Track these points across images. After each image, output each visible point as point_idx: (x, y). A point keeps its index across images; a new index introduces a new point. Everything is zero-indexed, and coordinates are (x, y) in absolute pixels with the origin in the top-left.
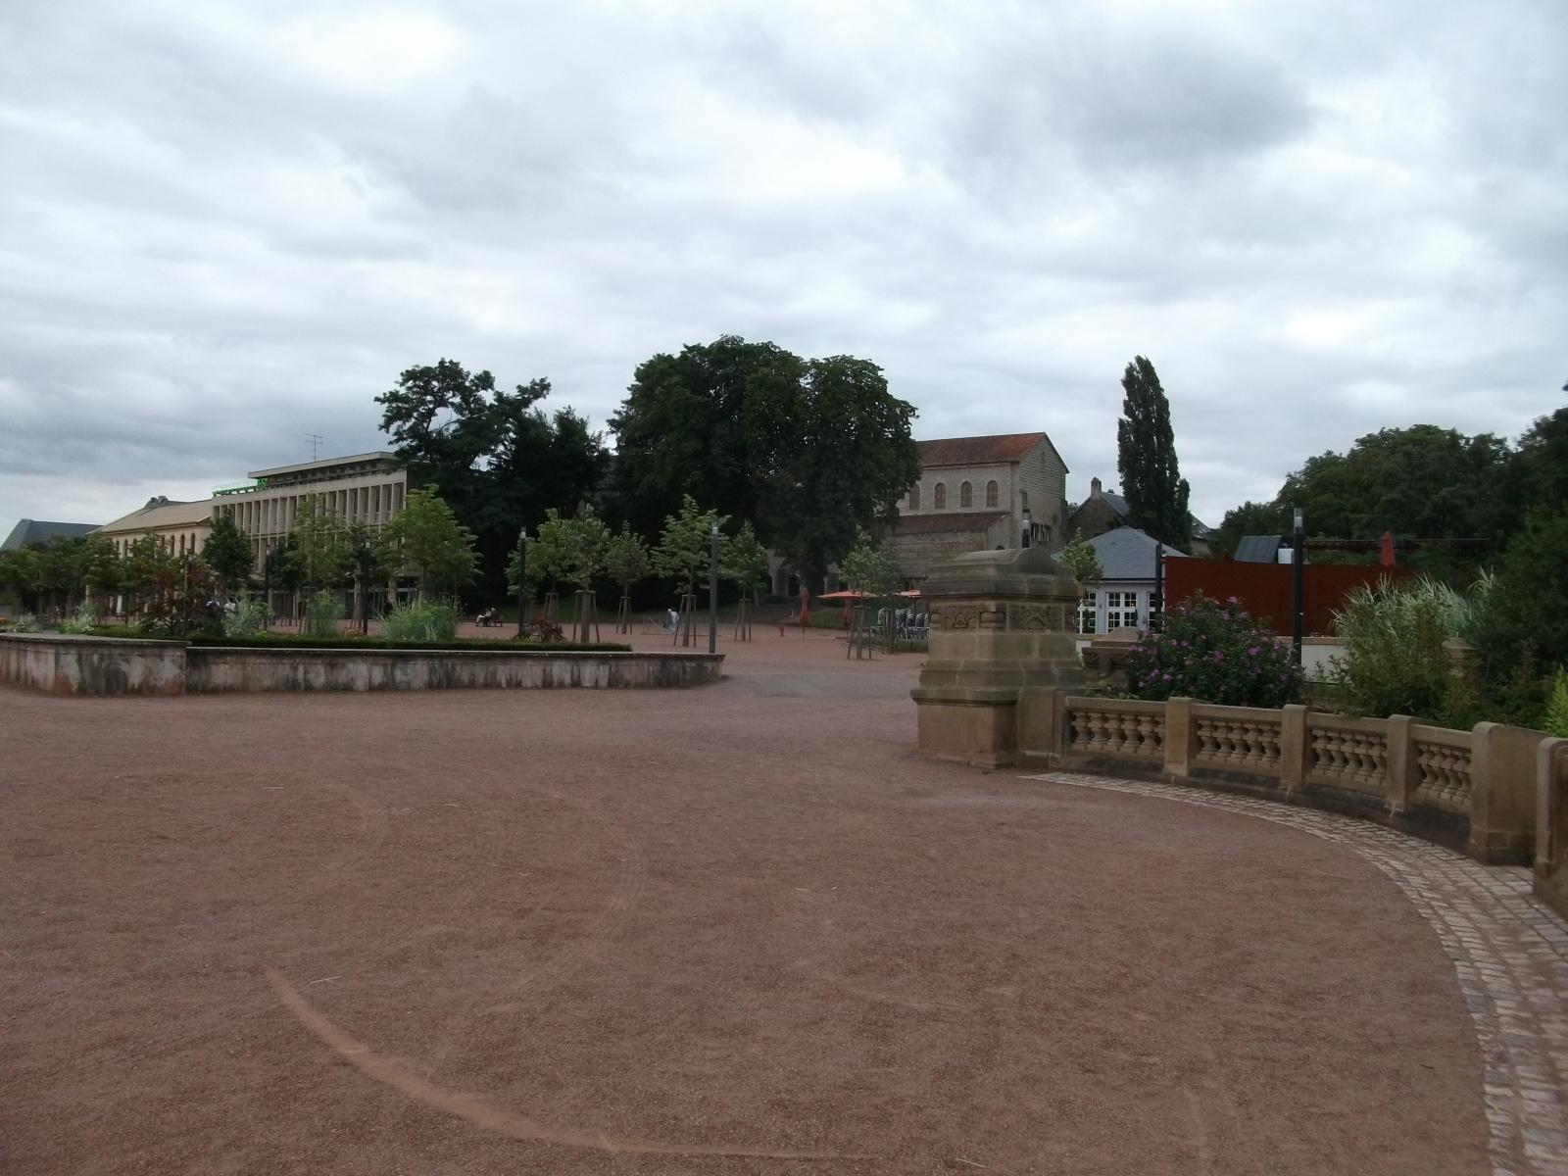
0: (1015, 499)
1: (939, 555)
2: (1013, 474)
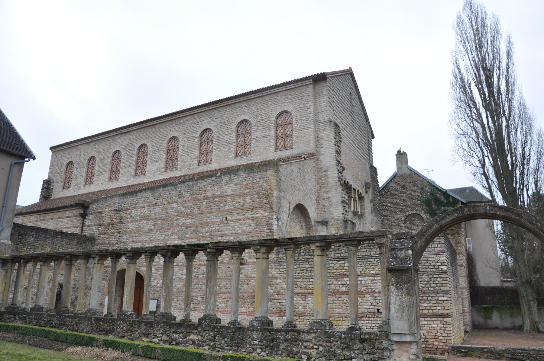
1: (189, 221)
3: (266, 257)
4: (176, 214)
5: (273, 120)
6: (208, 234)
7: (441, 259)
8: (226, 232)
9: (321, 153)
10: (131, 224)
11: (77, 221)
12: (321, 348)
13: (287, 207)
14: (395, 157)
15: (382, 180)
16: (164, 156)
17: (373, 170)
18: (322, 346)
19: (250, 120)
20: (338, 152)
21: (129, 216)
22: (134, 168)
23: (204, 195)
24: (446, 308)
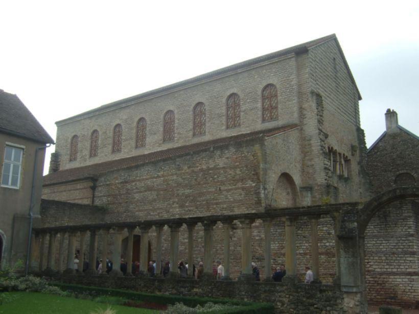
0: (305, 105)
1: (187, 191)
2: (299, 68)
3: (249, 227)
4: (176, 185)
5: (259, 93)
6: (205, 202)
7: (408, 223)
8: (220, 201)
9: (305, 123)
10: (137, 194)
11: (88, 193)
12: (291, 297)
13: (273, 177)
14: (383, 118)
15: (370, 142)
16: (162, 129)
17: (360, 133)
18: (292, 295)
19: (239, 93)
20: (320, 122)
21: (135, 188)
22: (134, 140)
23: (199, 168)
24: (413, 267)
